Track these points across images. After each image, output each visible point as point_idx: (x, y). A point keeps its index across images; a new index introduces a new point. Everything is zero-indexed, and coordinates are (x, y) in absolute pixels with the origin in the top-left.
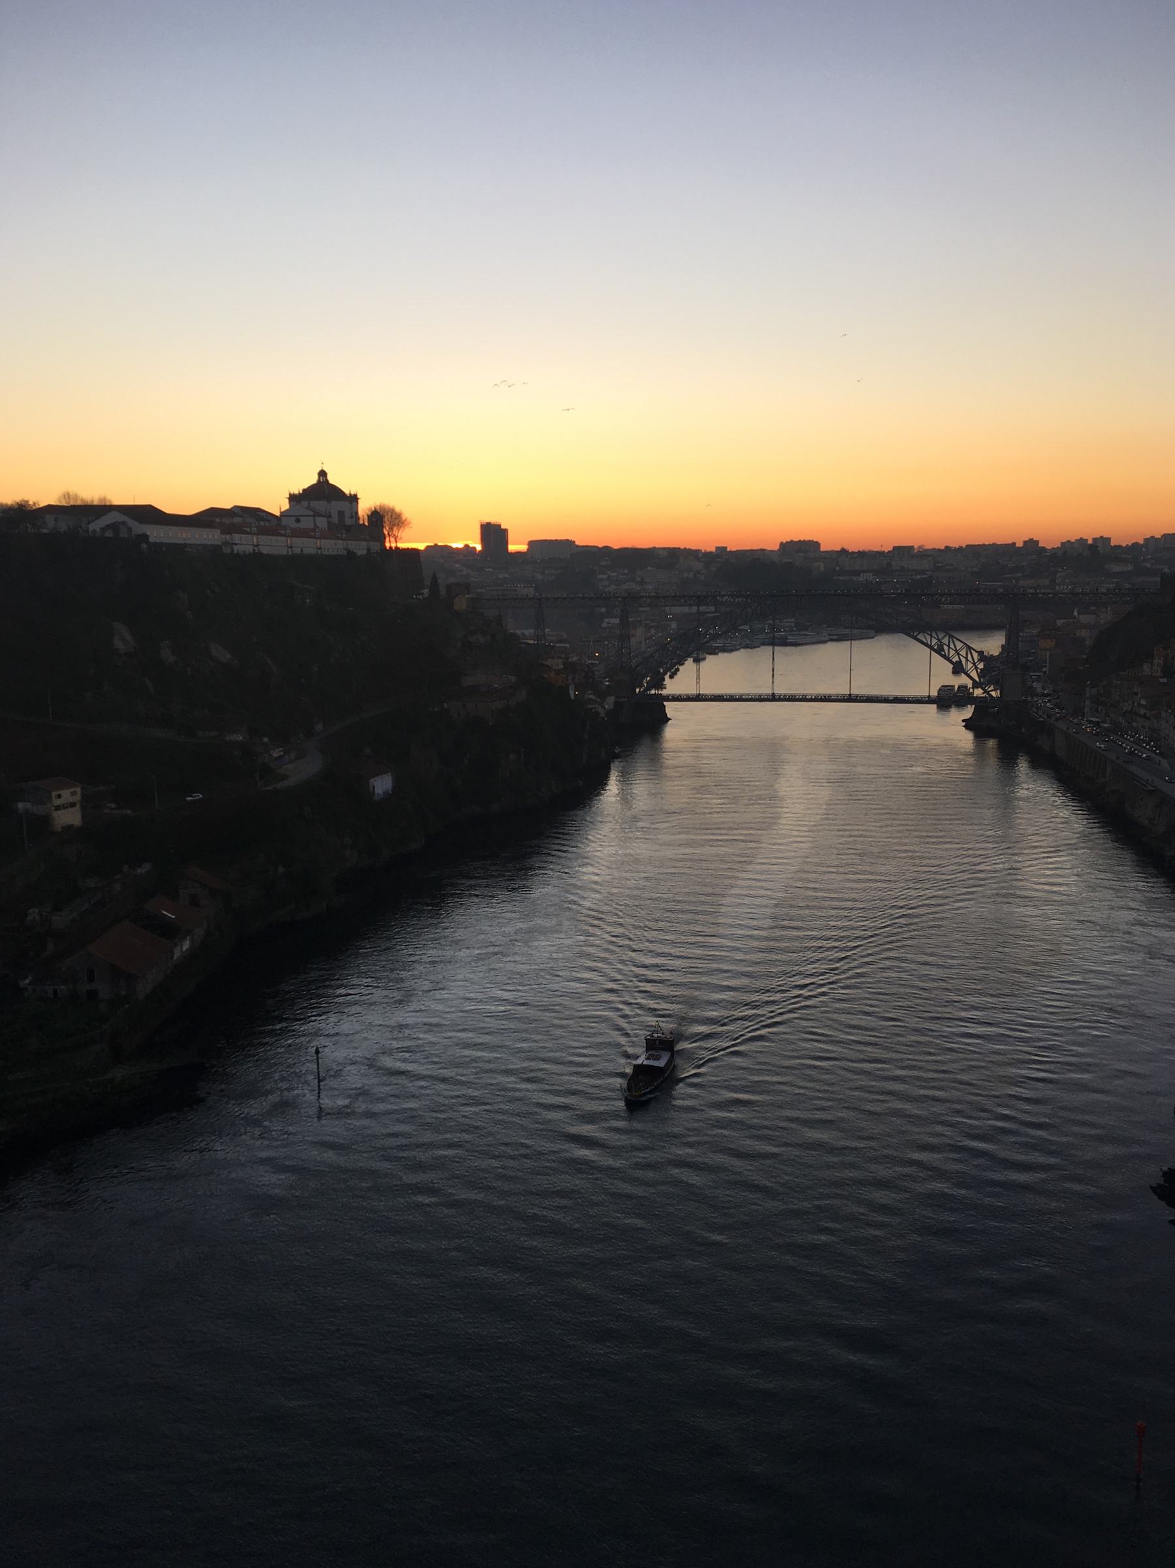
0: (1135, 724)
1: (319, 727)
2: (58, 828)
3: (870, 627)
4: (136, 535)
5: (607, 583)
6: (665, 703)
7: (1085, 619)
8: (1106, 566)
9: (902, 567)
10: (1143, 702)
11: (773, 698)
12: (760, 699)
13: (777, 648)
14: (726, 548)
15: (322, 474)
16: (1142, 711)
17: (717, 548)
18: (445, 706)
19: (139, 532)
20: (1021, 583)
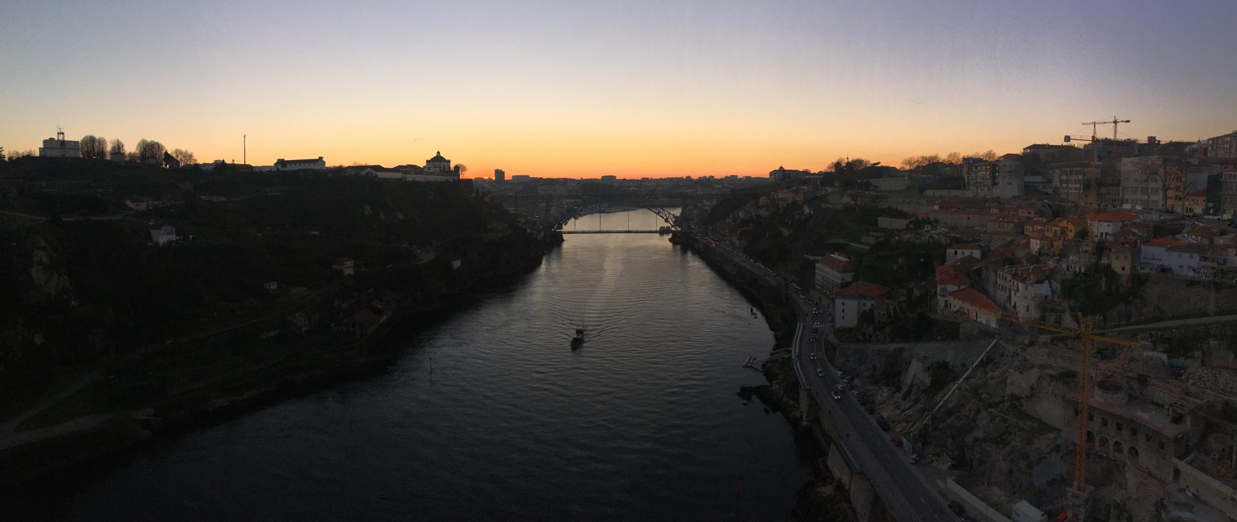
3: (634, 206)
7: (707, 203)
11: (600, 232)
12: (596, 232)
13: (602, 214)
15: (438, 153)
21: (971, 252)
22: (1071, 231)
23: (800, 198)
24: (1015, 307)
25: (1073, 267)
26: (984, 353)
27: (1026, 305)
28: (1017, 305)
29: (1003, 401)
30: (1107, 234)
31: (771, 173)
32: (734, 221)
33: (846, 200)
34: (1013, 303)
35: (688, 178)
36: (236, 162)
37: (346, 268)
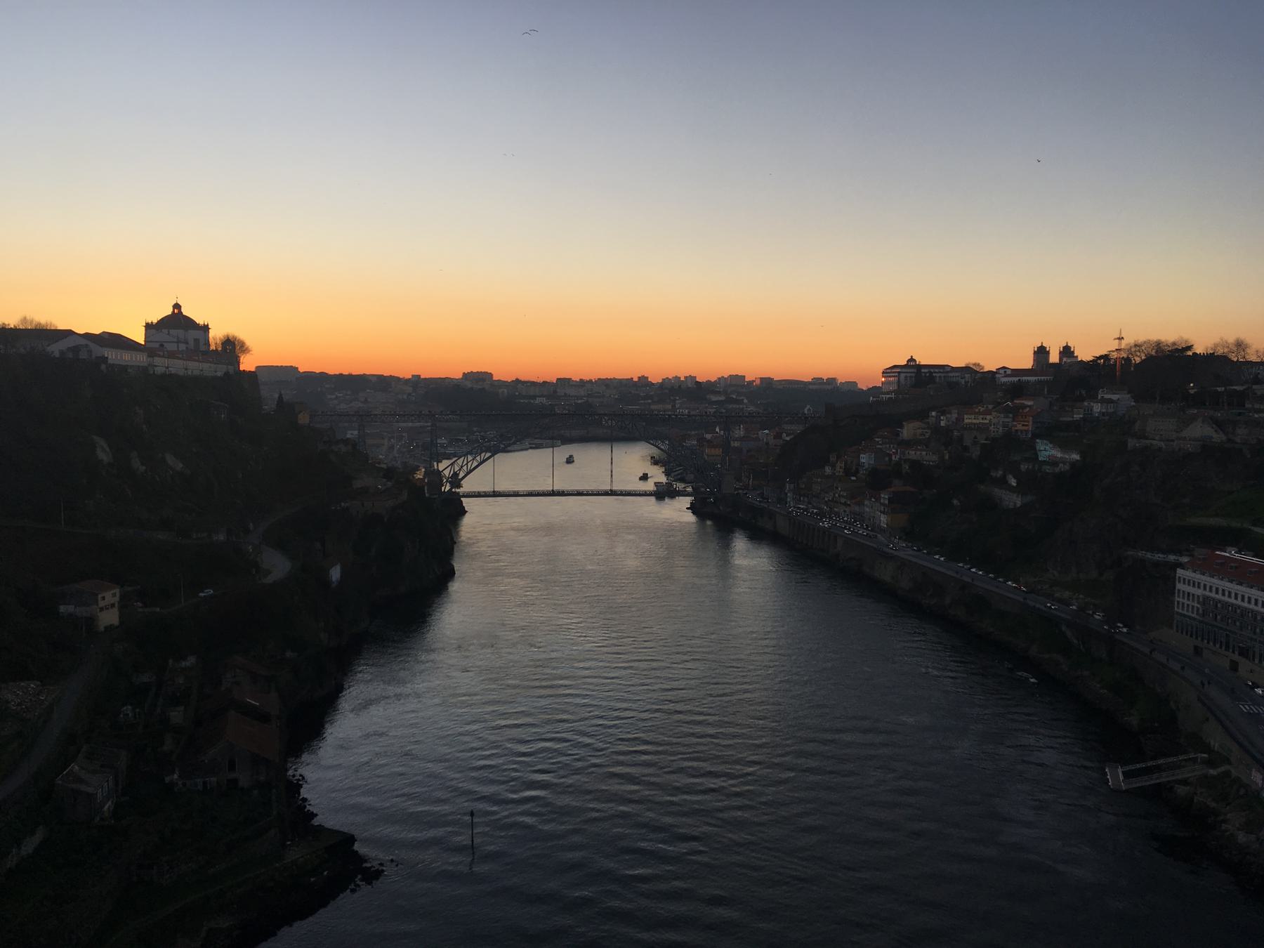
0: (835, 509)
1: (251, 526)
2: (102, 629)
3: (552, 438)
4: (96, 357)
5: (336, 402)
6: (462, 499)
8: (708, 397)
9: (565, 393)
14: (420, 376)
15: (177, 306)
16: (843, 500)
17: (413, 376)
18: (343, 504)
19: (99, 355)
20: (653, 407)
23: (1024, 427)
32: (848, 472)
33: (1200, 430)
35: (643, 380)
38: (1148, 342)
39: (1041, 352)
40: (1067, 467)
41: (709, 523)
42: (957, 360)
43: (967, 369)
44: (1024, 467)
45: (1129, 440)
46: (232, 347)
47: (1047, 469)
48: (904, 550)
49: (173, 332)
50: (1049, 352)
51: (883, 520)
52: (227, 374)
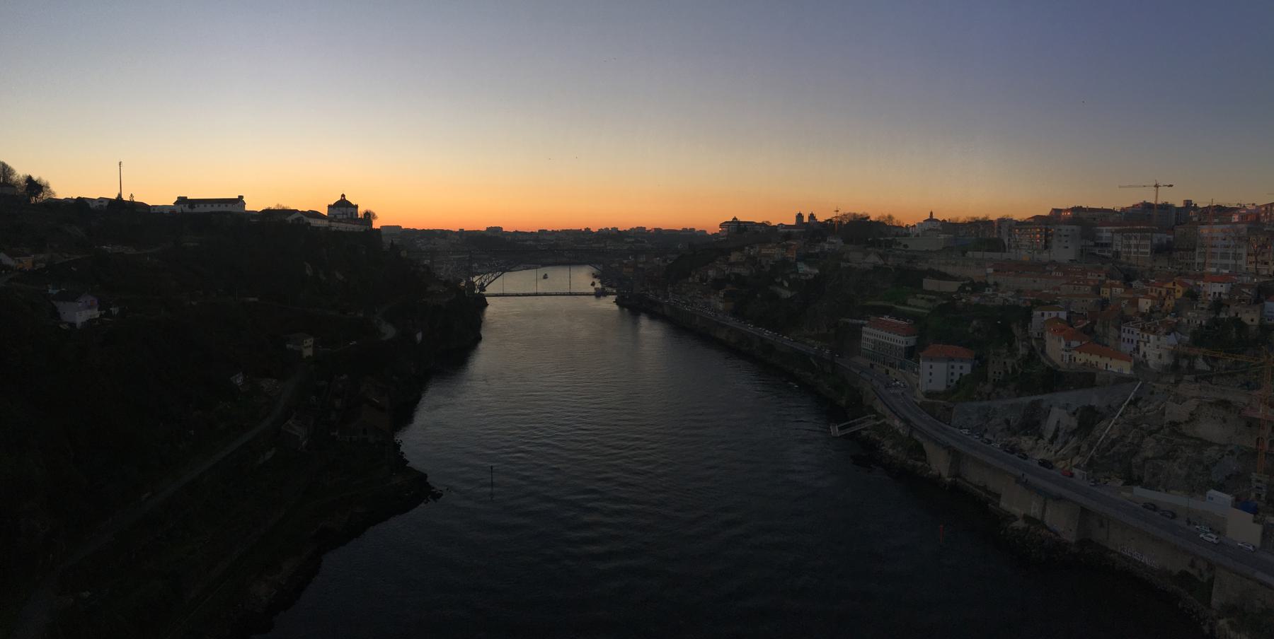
0: (695, 301)
10: (700, 292)
16: (699, 296)
21: (1058, 314)
22: (1179, 291)
23: (792, 256)
24: (1144, 356)
25: (1194, 322)
26: (1133, 393)
27: (1159, 353)
28: (1147, 354)
29: (1162, 427)
30: (1220, 294)
31: (721, 226)
32: (702, 280)
33: (873, 259)
34: (1141, 353)
36: (136, 200)
37: (305, 348)
38: (849, 214)
39: (800, 216)
40: (813, 276)
41: (626, 310)
42: (758, 220)
43: (763, 224)
44: (791, 277)
45: (842, 263)
46: (369, 216)
47: (803, 277)
48: (732, 322)
49: (341, 209)
50: (803, 217)
51: (721, 306)
52: (366, 230)
